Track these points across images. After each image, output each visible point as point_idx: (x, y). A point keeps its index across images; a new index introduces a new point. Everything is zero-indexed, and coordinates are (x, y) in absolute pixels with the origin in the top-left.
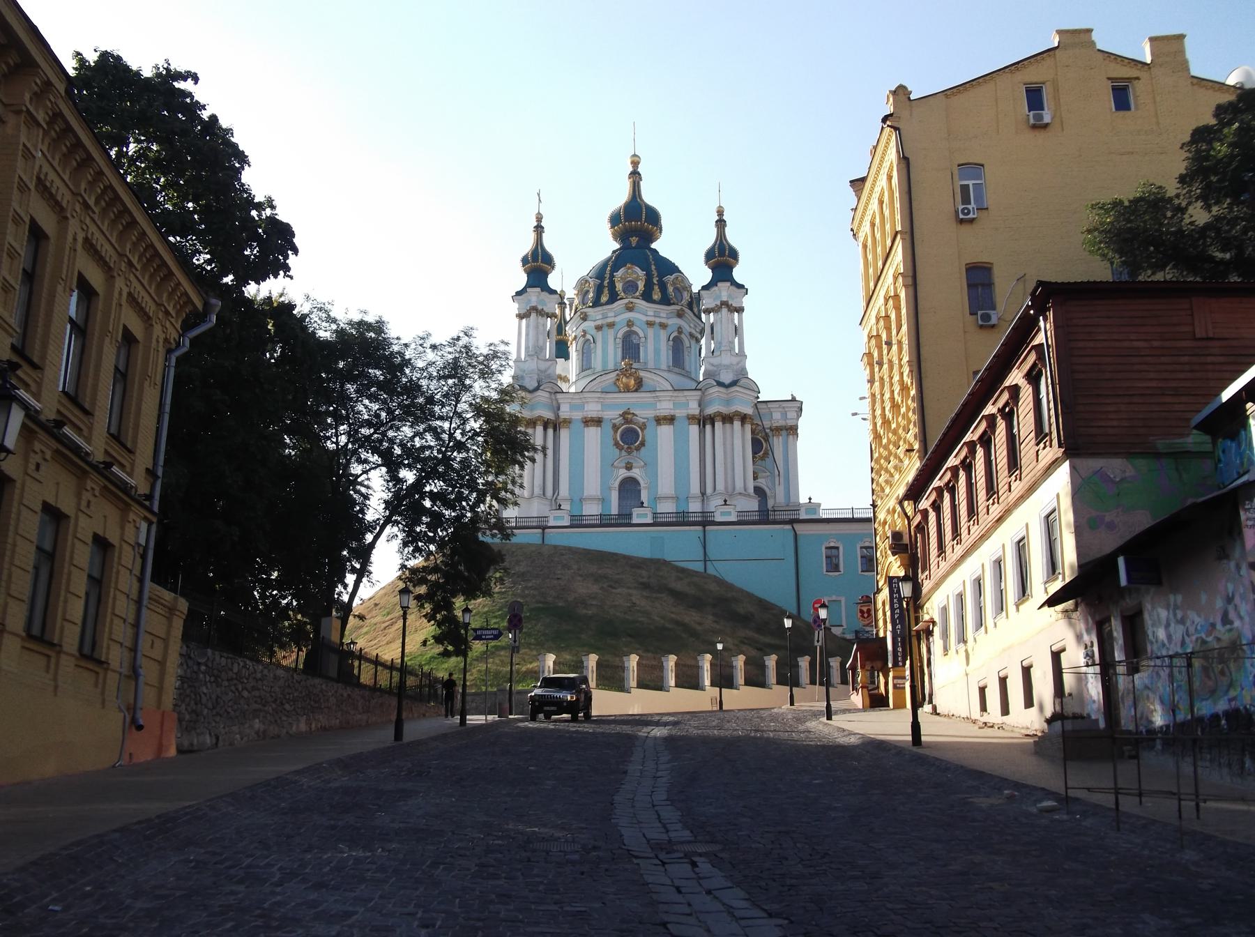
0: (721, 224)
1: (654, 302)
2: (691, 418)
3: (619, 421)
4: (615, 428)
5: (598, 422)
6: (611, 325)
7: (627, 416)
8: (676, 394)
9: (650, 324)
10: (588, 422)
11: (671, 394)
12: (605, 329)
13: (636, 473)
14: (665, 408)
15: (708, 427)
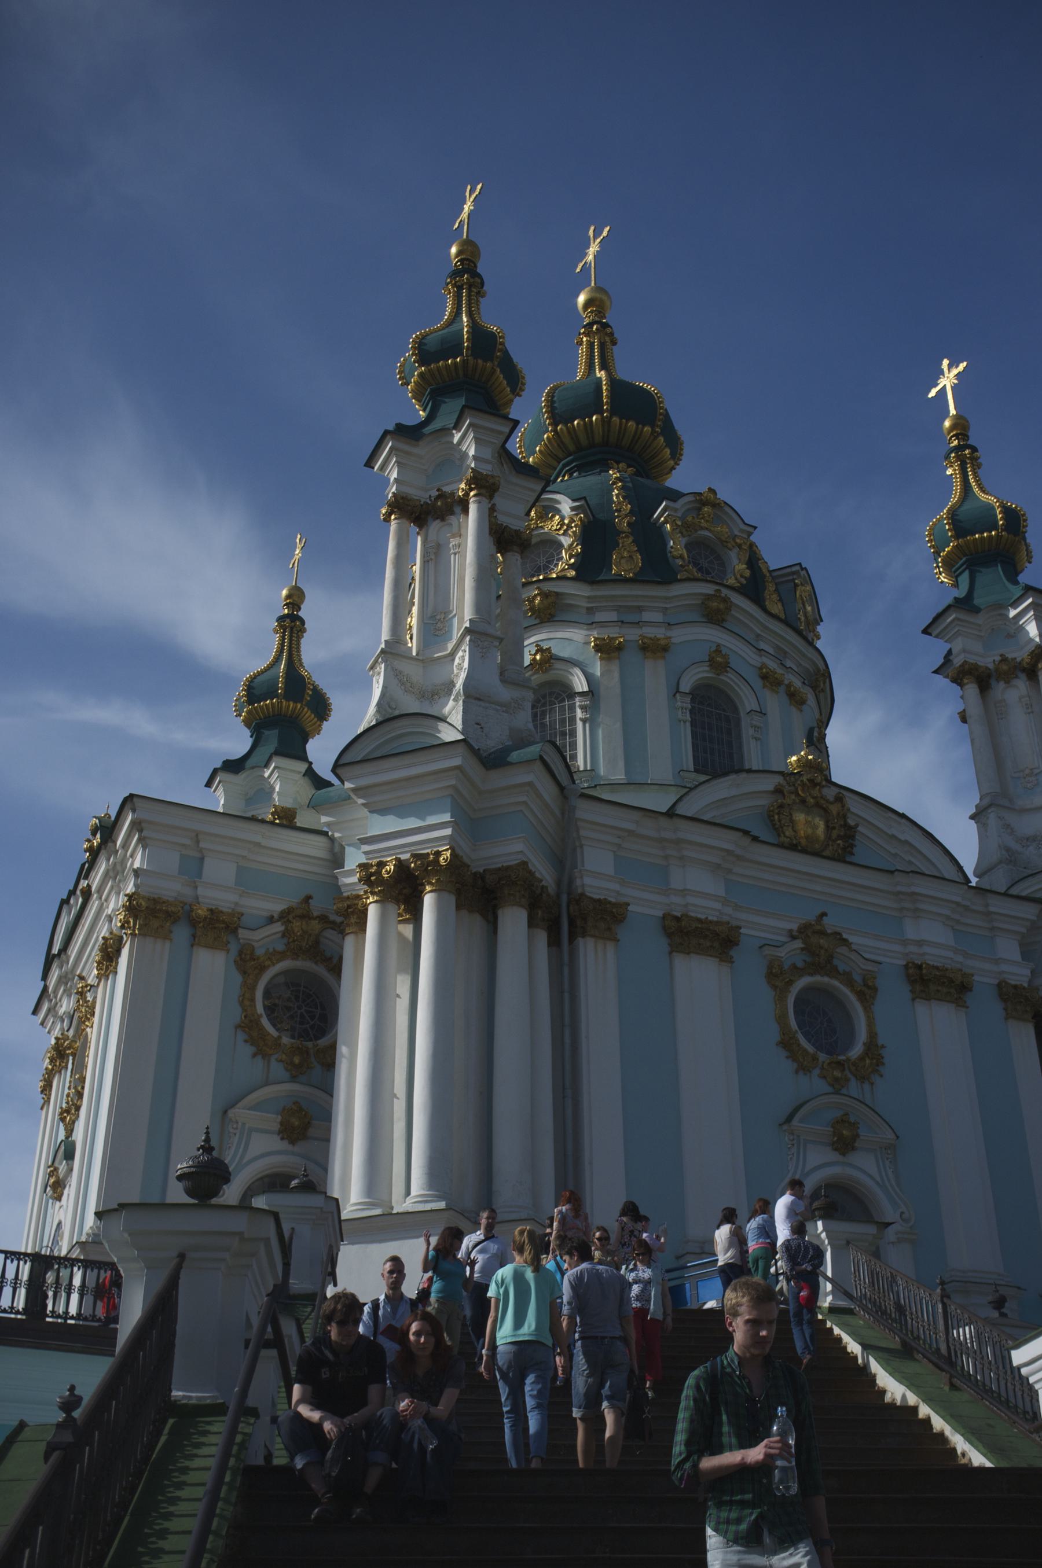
2: (1012, 997)
3: (791, 952)
4: (778, 976)
10: (688, 934)
13: (864, 1169)
14: (934, 940)
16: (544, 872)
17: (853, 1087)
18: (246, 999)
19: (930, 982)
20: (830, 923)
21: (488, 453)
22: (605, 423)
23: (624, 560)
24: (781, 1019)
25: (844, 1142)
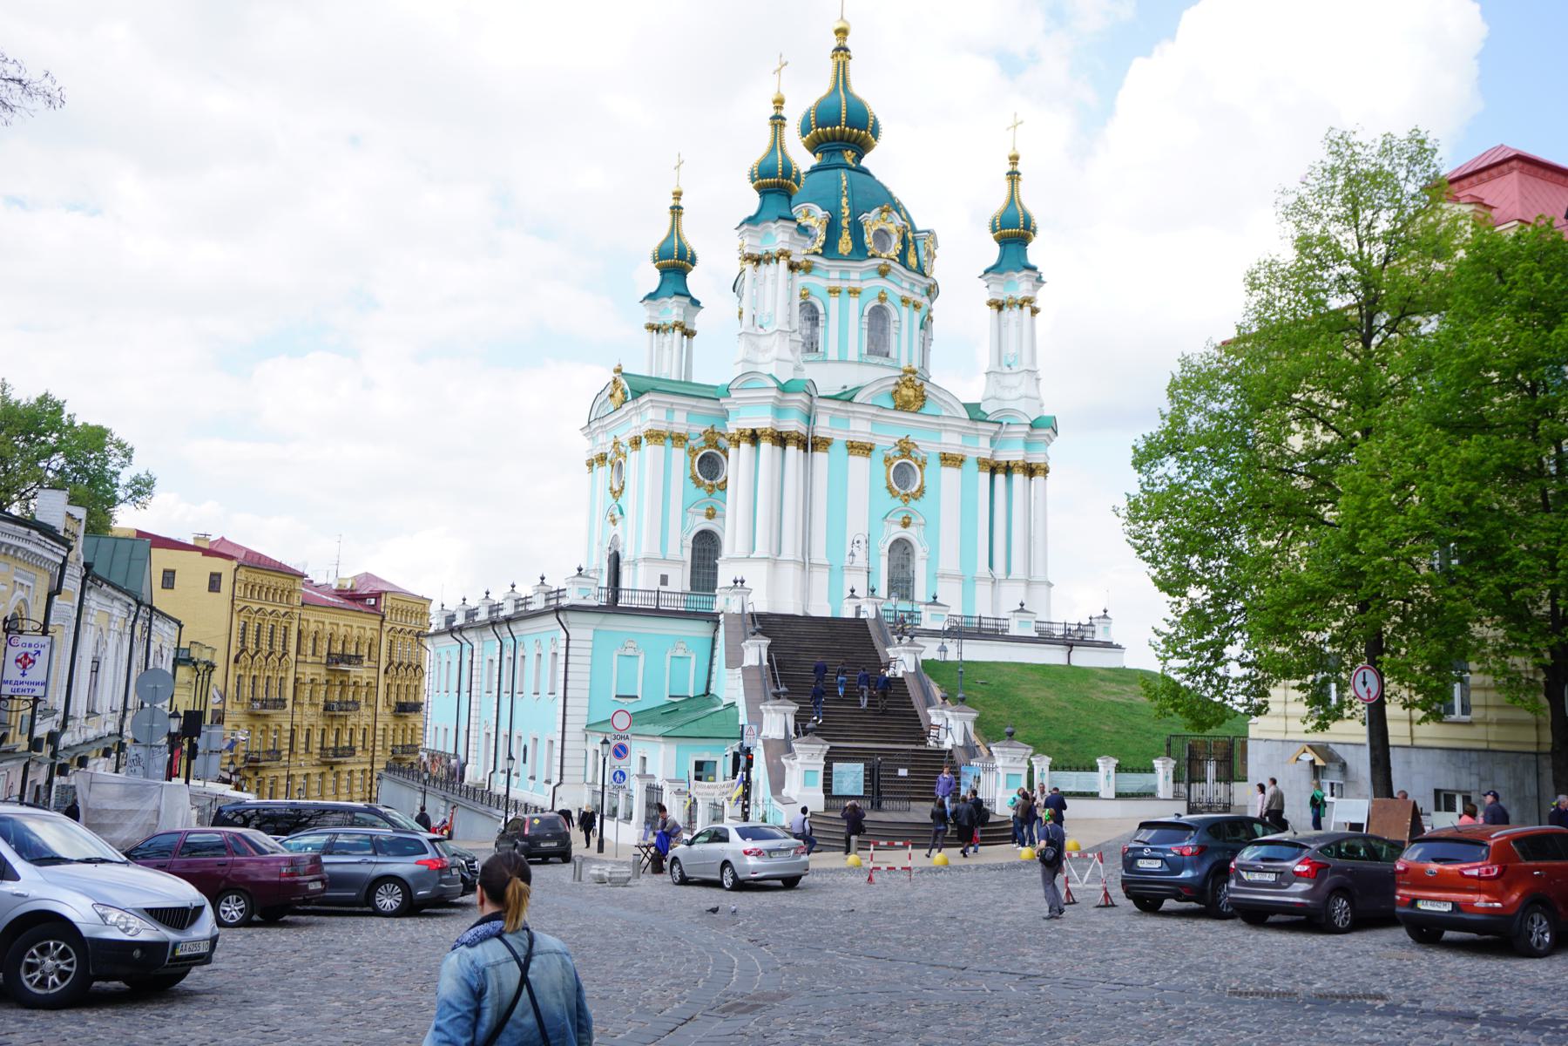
0: (1014, 176)
1: (910, 269)
2: (982, 463)
3: (895, 452)
4: (887, 460)
5: (866, 449)
6: (854, 292)
7: (905, 448)
8: (970, 424)
9: (905, 301)
10: (853, 447)
11: (964, 424)
12: (845, 295)
13: (910, 534)
14: (952, 442)
15: (1000, 478)
16: (803, 430)
17: (913, 503)
18: (692, 467)
19: (946, 459)
20: (911, 439)
21: (786, 237)
22: (843, 132)
23: (845, 244)
24: (888, 479)
25: (906, 524)
